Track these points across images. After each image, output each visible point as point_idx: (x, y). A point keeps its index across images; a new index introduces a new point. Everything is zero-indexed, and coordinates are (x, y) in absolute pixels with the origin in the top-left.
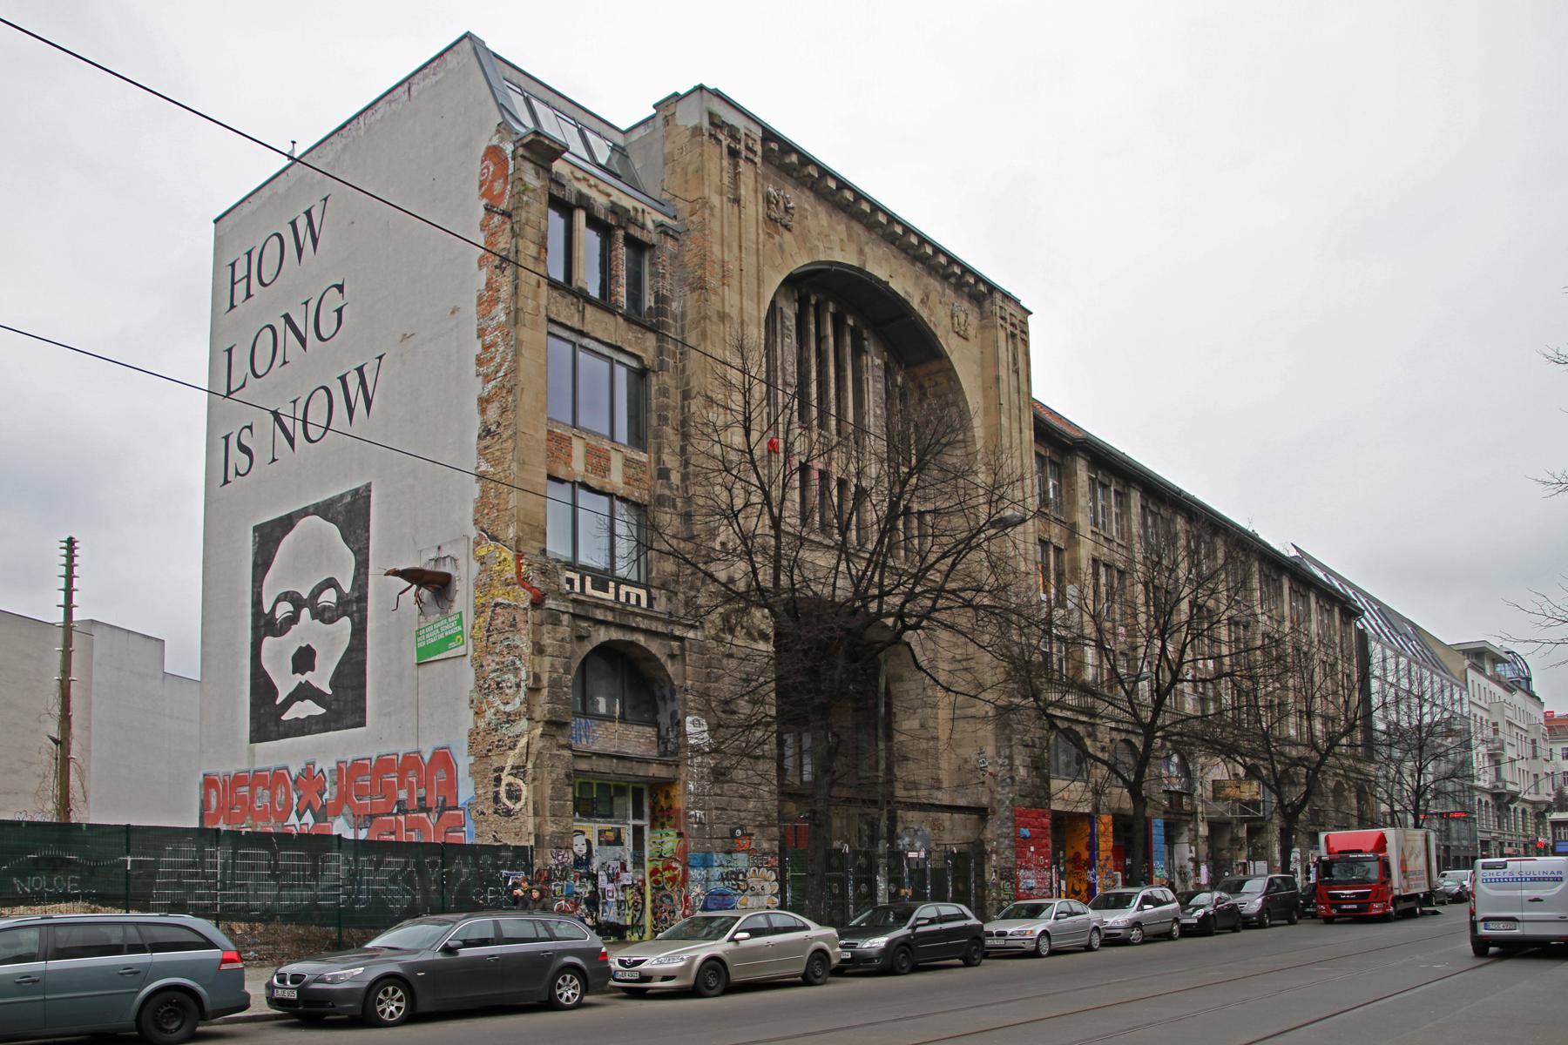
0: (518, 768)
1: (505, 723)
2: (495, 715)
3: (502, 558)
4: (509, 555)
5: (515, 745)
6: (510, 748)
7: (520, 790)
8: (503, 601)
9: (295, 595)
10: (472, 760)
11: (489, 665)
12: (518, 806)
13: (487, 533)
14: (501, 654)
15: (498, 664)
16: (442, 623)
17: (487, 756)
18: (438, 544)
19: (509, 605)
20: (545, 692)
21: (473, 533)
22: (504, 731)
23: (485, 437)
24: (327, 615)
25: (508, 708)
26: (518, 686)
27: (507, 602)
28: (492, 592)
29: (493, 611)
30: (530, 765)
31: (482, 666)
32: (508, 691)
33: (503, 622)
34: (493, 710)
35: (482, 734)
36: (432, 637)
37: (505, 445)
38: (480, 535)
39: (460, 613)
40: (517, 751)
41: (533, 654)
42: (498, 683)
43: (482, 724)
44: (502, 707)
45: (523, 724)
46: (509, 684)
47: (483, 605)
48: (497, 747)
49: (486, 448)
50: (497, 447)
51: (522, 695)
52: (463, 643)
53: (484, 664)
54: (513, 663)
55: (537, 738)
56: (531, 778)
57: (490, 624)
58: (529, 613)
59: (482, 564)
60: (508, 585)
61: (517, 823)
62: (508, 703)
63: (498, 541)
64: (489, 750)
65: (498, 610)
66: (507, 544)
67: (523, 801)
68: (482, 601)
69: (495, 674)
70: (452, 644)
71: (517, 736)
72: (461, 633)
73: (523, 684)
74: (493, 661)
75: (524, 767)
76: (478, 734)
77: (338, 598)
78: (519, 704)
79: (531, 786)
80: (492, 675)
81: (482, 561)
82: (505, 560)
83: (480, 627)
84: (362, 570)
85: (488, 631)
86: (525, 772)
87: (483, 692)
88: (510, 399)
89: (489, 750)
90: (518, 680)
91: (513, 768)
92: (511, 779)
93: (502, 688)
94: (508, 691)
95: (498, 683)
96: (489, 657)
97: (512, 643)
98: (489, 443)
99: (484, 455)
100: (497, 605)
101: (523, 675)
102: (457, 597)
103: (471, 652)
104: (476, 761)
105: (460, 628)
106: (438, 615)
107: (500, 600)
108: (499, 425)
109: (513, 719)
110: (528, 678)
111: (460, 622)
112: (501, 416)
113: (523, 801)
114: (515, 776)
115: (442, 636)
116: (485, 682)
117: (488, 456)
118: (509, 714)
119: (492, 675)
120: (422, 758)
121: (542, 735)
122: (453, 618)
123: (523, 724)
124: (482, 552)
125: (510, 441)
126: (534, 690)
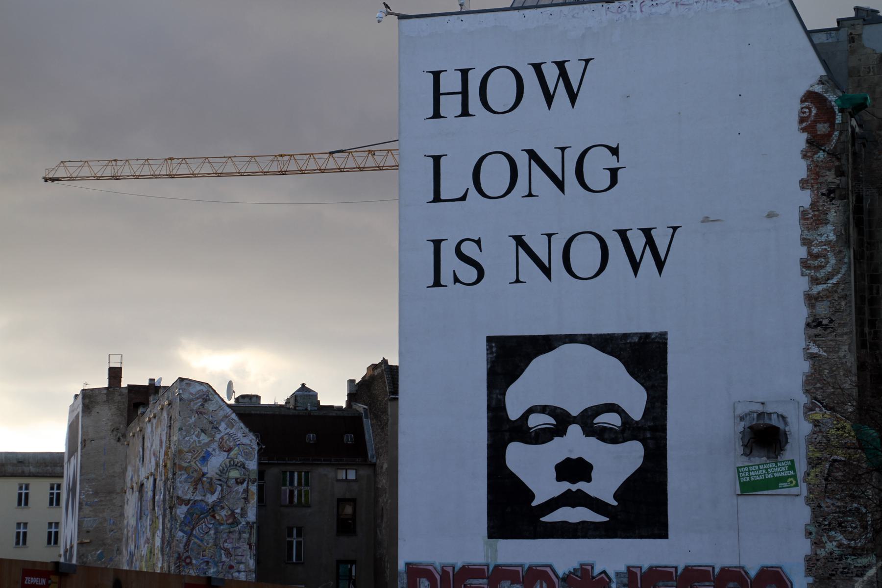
1: (850, 555)
6: (857, 576)
9: (558, 411)
10: (811, 580)
13: (822, 404)
15: (838, 507)
16: (770, 465)
17: (829, 578)
21: (804, 399)
22: (849, 561)
23: (816, 327)
24: (606, 436)
29: (831, 465)
31: (820, 506)
34: (835, 543)
35: (823, 560)
36: (758, 475)
37: (838, 338)
38: (813, 403)
39: (792, 461)
40: (865, 578)
43: (822, 553)
44: (845, 542)
47: (819, 459)
48: (842, 573)
49: (816, 336)
50: (830, 338)
52: (796, 485)
59: (816, 426)
64: (833, 575)
65: (836, 464)
68: (818, 455)
70: (785, 485)
71: (865, 567)
72: (795, 477)
76: (818, 560)
77: (623, 423)
81: (816, 423)
83: (816, 476)
84: (658, 404)
89: (833, 575)
95: (840, 524)
98: (820, 333)
99: (815, 342)
100: (835, 461)
102: (788, 447)
103: (805, 492)
104: (816, 582)
105: (792, 473)
106: (765, 459)
108: (831, 321)
111: (792, 467)
112: (833, 314)
115: (770, 476)
116: (824, 520)
117: (820, 342)
118: (855, 548)
120: (746, 573)
124: (818, 417)
125: (845, 337)
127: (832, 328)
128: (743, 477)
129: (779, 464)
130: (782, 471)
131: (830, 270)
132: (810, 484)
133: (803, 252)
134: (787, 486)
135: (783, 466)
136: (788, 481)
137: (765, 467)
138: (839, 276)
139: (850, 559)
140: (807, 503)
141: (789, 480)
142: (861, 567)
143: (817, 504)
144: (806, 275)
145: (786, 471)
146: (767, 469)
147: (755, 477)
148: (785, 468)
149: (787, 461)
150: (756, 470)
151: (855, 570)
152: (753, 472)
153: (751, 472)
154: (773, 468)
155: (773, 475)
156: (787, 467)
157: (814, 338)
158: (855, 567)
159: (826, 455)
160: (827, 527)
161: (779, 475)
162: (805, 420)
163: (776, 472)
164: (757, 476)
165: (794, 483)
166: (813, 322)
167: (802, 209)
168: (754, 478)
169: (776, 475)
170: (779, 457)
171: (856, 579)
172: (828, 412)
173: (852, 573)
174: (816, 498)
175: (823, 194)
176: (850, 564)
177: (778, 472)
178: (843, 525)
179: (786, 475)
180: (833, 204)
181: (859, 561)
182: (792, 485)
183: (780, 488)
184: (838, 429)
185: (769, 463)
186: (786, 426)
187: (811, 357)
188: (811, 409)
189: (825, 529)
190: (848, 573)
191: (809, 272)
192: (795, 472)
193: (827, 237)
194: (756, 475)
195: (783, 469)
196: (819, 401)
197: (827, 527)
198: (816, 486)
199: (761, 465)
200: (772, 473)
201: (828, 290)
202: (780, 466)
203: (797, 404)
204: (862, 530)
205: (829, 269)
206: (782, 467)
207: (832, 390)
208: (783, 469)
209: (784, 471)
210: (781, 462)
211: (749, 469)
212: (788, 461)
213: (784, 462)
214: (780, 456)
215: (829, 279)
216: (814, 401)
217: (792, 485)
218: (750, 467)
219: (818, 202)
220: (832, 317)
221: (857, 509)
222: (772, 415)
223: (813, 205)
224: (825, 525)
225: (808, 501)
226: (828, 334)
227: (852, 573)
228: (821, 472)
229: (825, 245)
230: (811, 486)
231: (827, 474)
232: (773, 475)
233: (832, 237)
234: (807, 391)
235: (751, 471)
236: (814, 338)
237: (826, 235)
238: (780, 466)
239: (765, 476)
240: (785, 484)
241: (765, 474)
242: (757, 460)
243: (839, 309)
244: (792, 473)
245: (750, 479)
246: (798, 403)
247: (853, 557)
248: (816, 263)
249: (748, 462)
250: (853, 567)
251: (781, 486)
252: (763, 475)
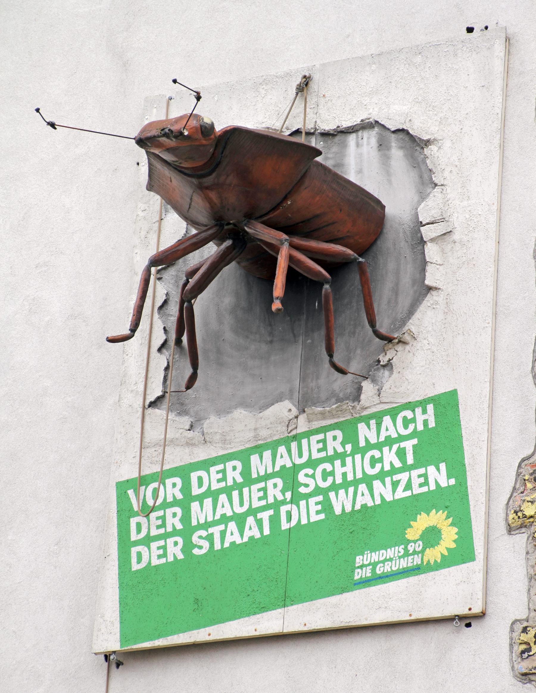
128: (148, 540)
130: (381, 476)
134: (404, 564)
135: (389, 442)
136: (412, 534)
140: (524, 666)
141: (421, 548)
145: (406, 468)
147: (216, 530)
148: (401, 454)
149: (411, 406)
150: (228, 491)
152: (208, 502)
153: (195, 506)
154: (330, 460)
156: (408, 445)
163: (346, 484)
164: (232, 526)
168: (210, 538)
170: (367, 386)
177: (356, 483)
179: (400, 494)
183: (365, 583)
185: (308, 434)
186: (423, 197)
194: (225, 519)
199: (259, 449)
200: (318, 491)
202: (369, 446)
203: (499, 48)
206: (379, 446)
209: (394, 471)
210: (379, 417)
211: (186, 488)
212: (423, 404)
213: (393, 413)
214: (374, 381)
218: (194, 476)
222: (352, 139)
235: (200, 498)
238: (369, 446)
239: (275, 521)
240: (390, 553)
241: (277, 505)
245: (188, 547)
246: (508, 39)
249: (190, 444)
251: (367, 573)
252: (265, 516)
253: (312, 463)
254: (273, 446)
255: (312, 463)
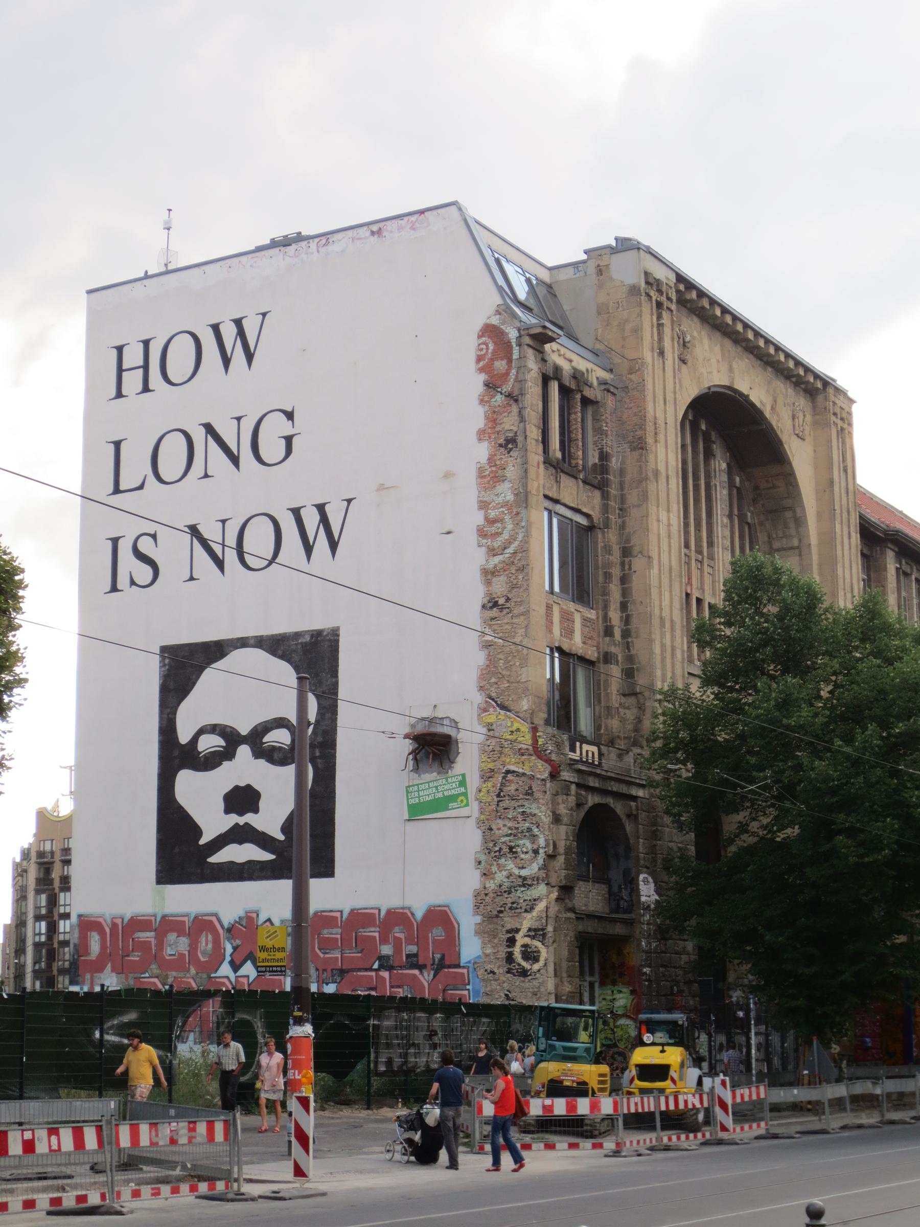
0: (535, 930)
1: (520, 886)
2: (508, 877)
3: (514, 728)
4: (525, 728)
5: (532, 908)
6: (526, 911)
7: (539, 952)
8: (516, 769)
11: (499, 829)
12: (536, 967)
13: (496, 702)
14: (514, 819)
15: (510, 828)
18: (434, 703)
19: (524, 774)
20: (561, 859)
21: (478, 698)
22: (519, 894)
23: (491, 608)
25: (524, 873)
26: (536, 852)
27: (521, 770)
28: (504, 759)
29: (504, 778)
30: (550, 929)
31: (491, 829)
32: (523, 856)
33: (517, 790)
34: (505, 873)
37: (515, 620)
38: (487, 702)
39: (463, 776)
41: (552, 823)
42: (511, 848)
45: (542, 889)
46: (524, 850)
47: (492, 770)
49: (492, 619)
50: (505, 621)
51: (540, 859)
52: (467, 805)
53: (494, 827)
54: (529, 830)
55: (553, 902)
56: (551, 941)
57: (501, 790)
58: (548, 785)
59: (489, 730)
60: (523, 755)
61: (535, 983)
62: (523, 868)
63: (510, 711)
65: (510, 777)
66: (521, 715)
67: (541, 962)
69: (508, 838)
70: (455, 805)
71: (535, 900)
72: (465, 794)
73: (541, 851)
74: (504, 825)
75: (543, 930)
78: (536, 869)
79: (551, 949)
80: (503, 839)
81: (490, 727)
82: (518, 730)
83: (488, 791)
85: (498, 795)
86: (544, 935)
87: (493, 854)
88: (520, 577)
90: (535, 847)
91: (530, 930)
92: (527, 940)
93: (516, 852)
94: (523, 856)
95: (511, 848)
96: (499, 821)
97: (528, 811)
101: (542, 842)
102: (459, 759)
103: (476, 813)
105: (463, 790)
107: (512, 768)
108: (508, 600)
109: (529, 883)
110: (547, 845)
111: (463, 783)
113: (541, 962)
114: (533, 938)
116: (495, 845)
117: (495, 627)
118: (525, 879)
119: (503, 839)
121: (557, 899)
122: (454, 779)
123: (542, 889)
124: (492, 718)
125: (522, 618)
126: (551, 857)
127: (508, 608)
129: (450, 780)
131: (506, 538)
132: (481, 802)
133: (478, 518)
137: (435, 784)
138: (516, 543)
139: (519, 892)
142: (530, 900)
143: (488, 826)
144: (482, 546)
146: (437, 787)
151: (524, 904)
155: (443, 794)
157: (490, 623)
158: (525, 900)
159: (498, 764)
160: (497, 854)
161: (450, 793)
162: (480, 724)
165: (465, 802)
166: (489, 602)
167: (479, 466)
169: (446, 793)
171: (525, 915)
172: (502, 712)
173: (521, 908)
174: (488, 819)
175: (501, 445)
176: (519, 897)
178: (514, 850)
180: (511, 457)
181: (529, 892)
182: (462, 805)
184: (512, 732)
187: (487, 646)
188: (485, 710)
189: (495, 856)
190: (517, 908)
191: (485, 541)
192: (466, 788)
193: (505, 497)
195: (454, 785)
196: (493, 700)
197: (497, 854)
198: (487, 804)
201: (504, 562)
204: (533, 855)
205: (506, 536)
207: (507, 685)
208: (454, 785)
215: (505, 548)
216: (488, 699)
217: (462, 805)
219: (495, 455)
220: (509, 595)
221: (529, 830)
223: (491, 460)
224: (495, 852)
225: (480, 823)
226: (504, 616)
227: (521, 908)
228: (493, 787)
229: (502, 507)
230: (482, 804)
231: (500, 789)
232: (443, 794)
233: (510, 497)
234: (481, 688)
236: (490, 623)
237: (503, 495)
242: (427, 777)
243: (516, 584)
244: (463, 790)
247: (523, 889)
248: (493, 530)
250: (522, 901)
253: (440, 785)
254: (433, 781)
255: (440, 785)
